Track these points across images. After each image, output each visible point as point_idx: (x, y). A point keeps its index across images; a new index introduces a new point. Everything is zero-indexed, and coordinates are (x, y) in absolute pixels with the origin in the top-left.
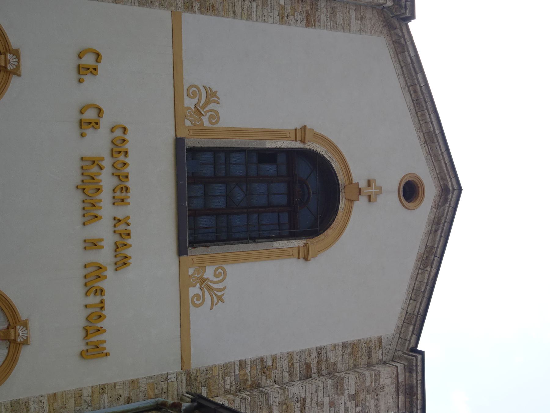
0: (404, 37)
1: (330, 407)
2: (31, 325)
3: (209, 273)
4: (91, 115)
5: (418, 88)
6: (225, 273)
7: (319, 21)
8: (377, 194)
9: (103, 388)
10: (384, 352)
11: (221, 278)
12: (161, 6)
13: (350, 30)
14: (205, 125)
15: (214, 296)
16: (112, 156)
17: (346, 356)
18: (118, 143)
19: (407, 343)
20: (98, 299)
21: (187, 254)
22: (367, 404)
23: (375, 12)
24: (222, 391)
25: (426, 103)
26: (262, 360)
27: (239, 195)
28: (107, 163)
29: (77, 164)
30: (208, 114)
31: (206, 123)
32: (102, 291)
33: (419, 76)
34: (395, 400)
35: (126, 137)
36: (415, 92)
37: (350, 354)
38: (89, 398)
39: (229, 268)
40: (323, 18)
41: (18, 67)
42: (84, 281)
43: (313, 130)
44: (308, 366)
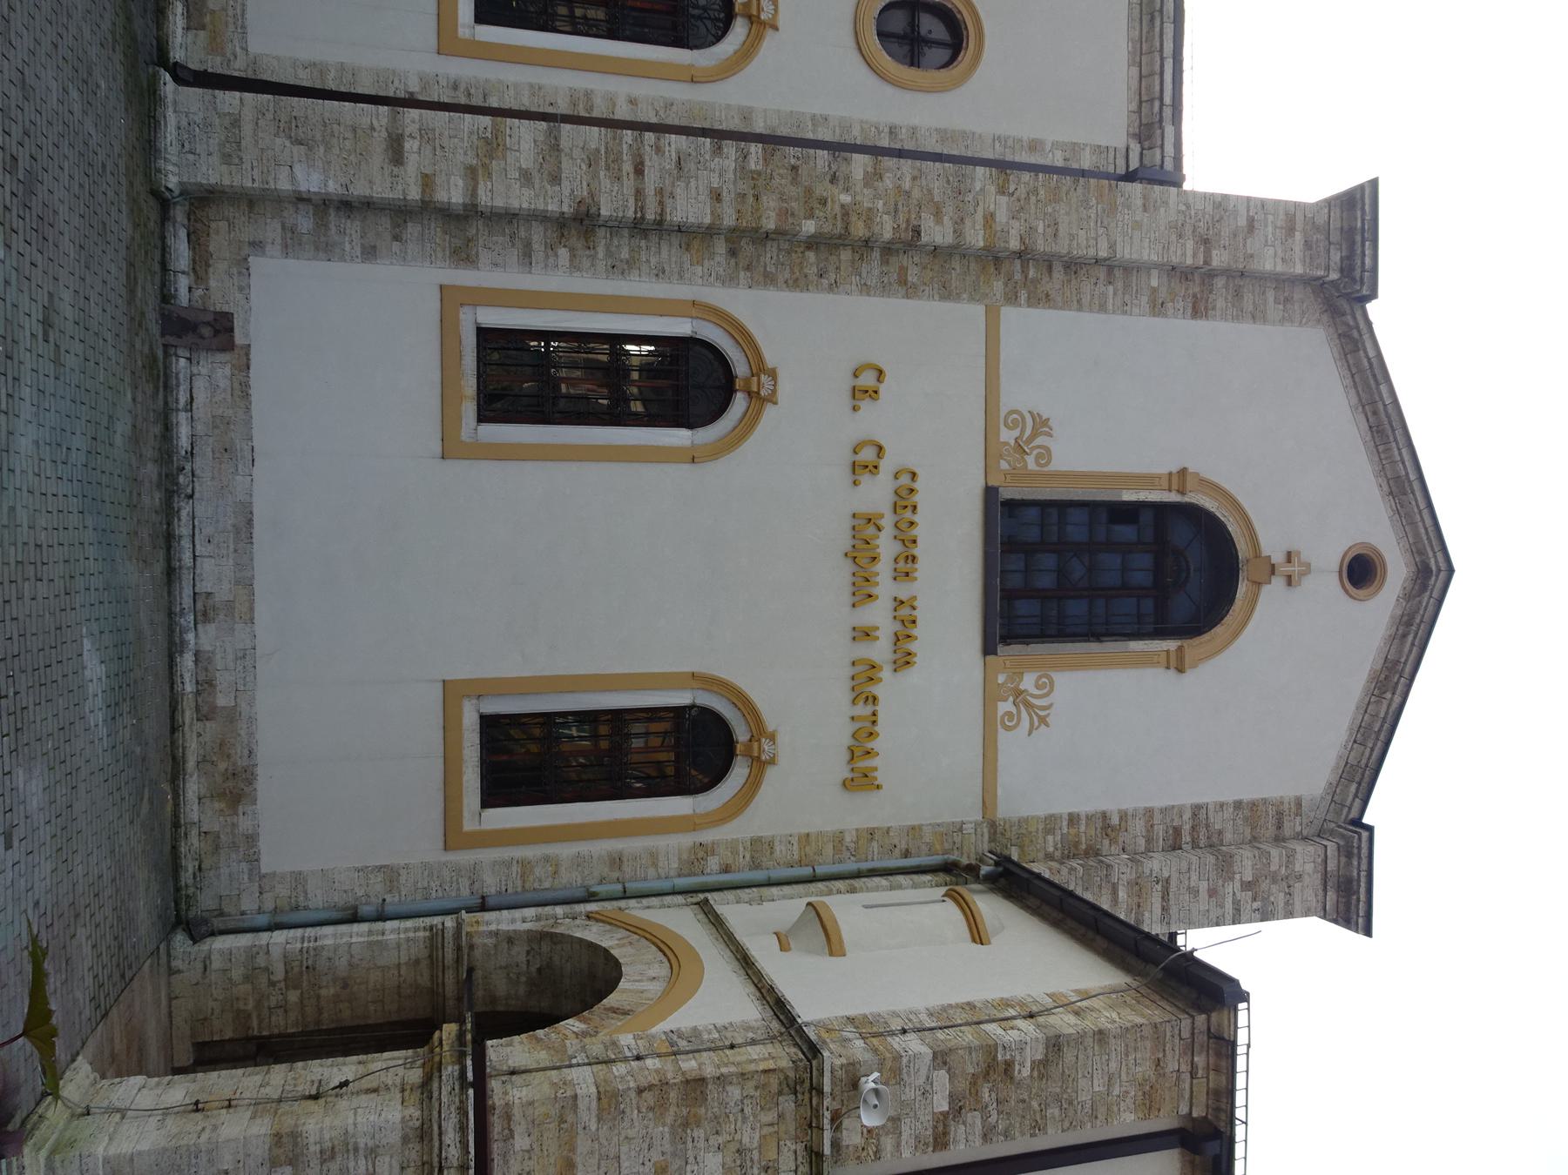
0: (1357, 328)
1: (1210, 896)
2: (779, 740)
3: (1028, 682)
4: (868, 455)
5: (1381, 407)
6: (1052, 684)
7: (1214, 308)
8: (1302, 574)
9: (872, 833)
10: (1305, 821)
11: (1045, 691)
12: (972, 299)
13: (1265, 321)
14: (1030, 467)
15: (1035, 718)
16: (895, 513)
17: (1240, 822)
18: (904, 493)
19: (1345, 810)
20: (869, 709)
21: (996, 654)
22: (1272, 899)
23: (1309, 289)
24: (1041, 855)
25: (1393, 431)
26: (1104, 816)
27: (1077, 570)
28: (887, 522)
29: (847, 523)
30: (1035, 452)
31: (1031, 465)
32: (875, 698)
33: (1383, 388)
34: (1320, 898)
35: (916, 486)
36: (1375, 413)
37: (1246, 819)
38: (853, 845)
39: (1063, 680)
40: (1220, 303)
41: (774, 391)
42: (849, 684)
43: (1198, 474)
44: (1177, 831)
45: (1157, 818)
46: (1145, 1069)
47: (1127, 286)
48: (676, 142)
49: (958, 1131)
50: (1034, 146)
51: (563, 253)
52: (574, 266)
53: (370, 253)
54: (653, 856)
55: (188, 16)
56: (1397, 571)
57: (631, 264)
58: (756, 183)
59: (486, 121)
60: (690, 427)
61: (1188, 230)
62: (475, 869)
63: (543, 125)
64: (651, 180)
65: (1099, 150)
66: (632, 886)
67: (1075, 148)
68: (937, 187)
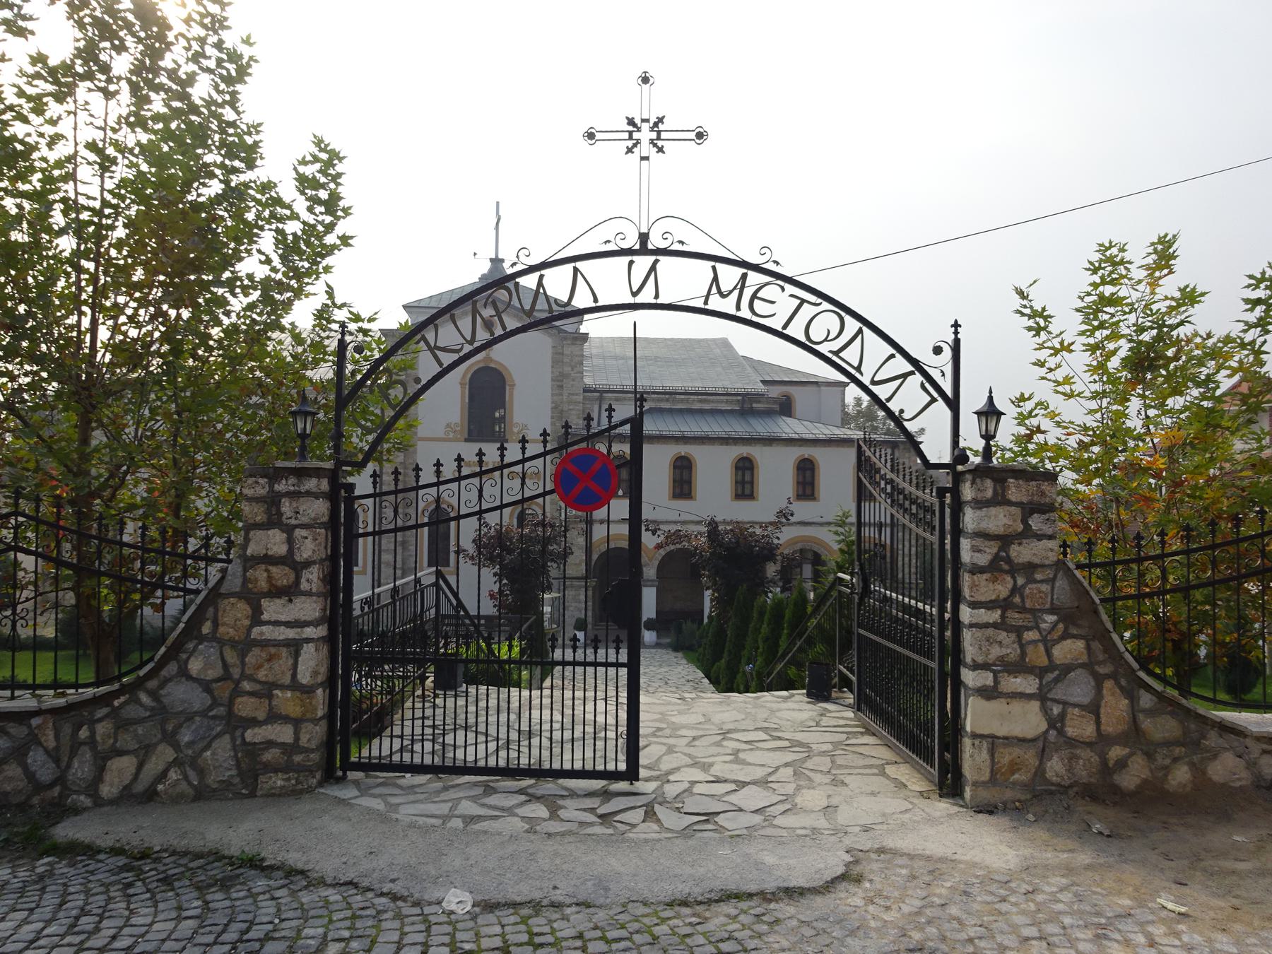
3: (516, 430)
39: (516, 420)
44: (558, 386)
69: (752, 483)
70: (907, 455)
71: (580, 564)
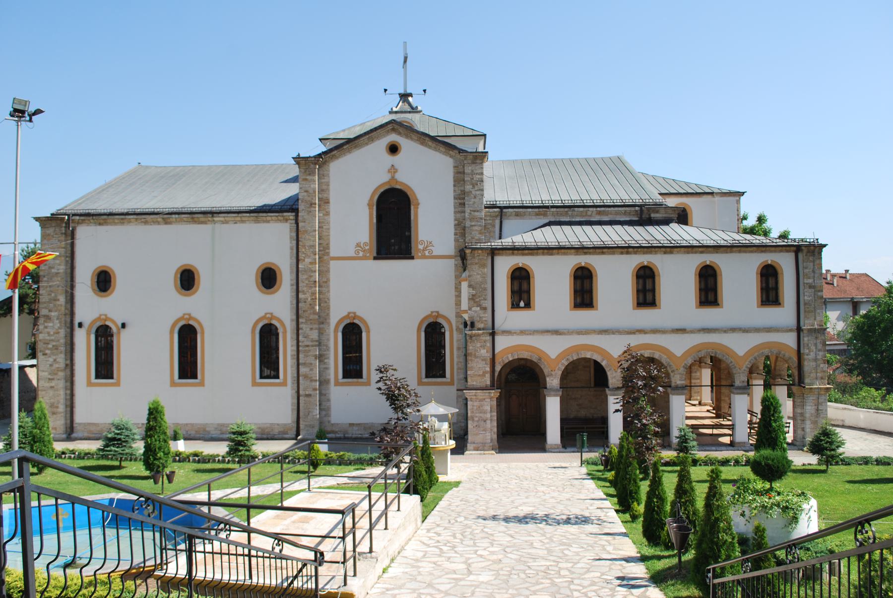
12: (329, 264)
13: (329, 182)
26: (455, 225)
37: (458, 183)
39: (420, 238)
40: (325, 195)
44: (460, 204)
45: (457, 210)
46: (477, 266)
47: (323, 222)
48: (301, 338)
49: (484, 305)
50: (292, 249)
51: (326, 361)
52: (328, 358)
53: (329, 400)
54: (458, 341)
55: (285, 434)
56: (393, 138)
57: (327, 346)
58: (308, 320)
59: (301, 378)
60: (361, 332)
61: (309, 209)
62: (458, 379)
63: (300, 366)
64: (310, 343)
65: (291, 231)
66: (464, 346)
67: (291, 238)
68: (305, 277)
69: (653, 290)
70: (811, 259)
71: (483, 375)
